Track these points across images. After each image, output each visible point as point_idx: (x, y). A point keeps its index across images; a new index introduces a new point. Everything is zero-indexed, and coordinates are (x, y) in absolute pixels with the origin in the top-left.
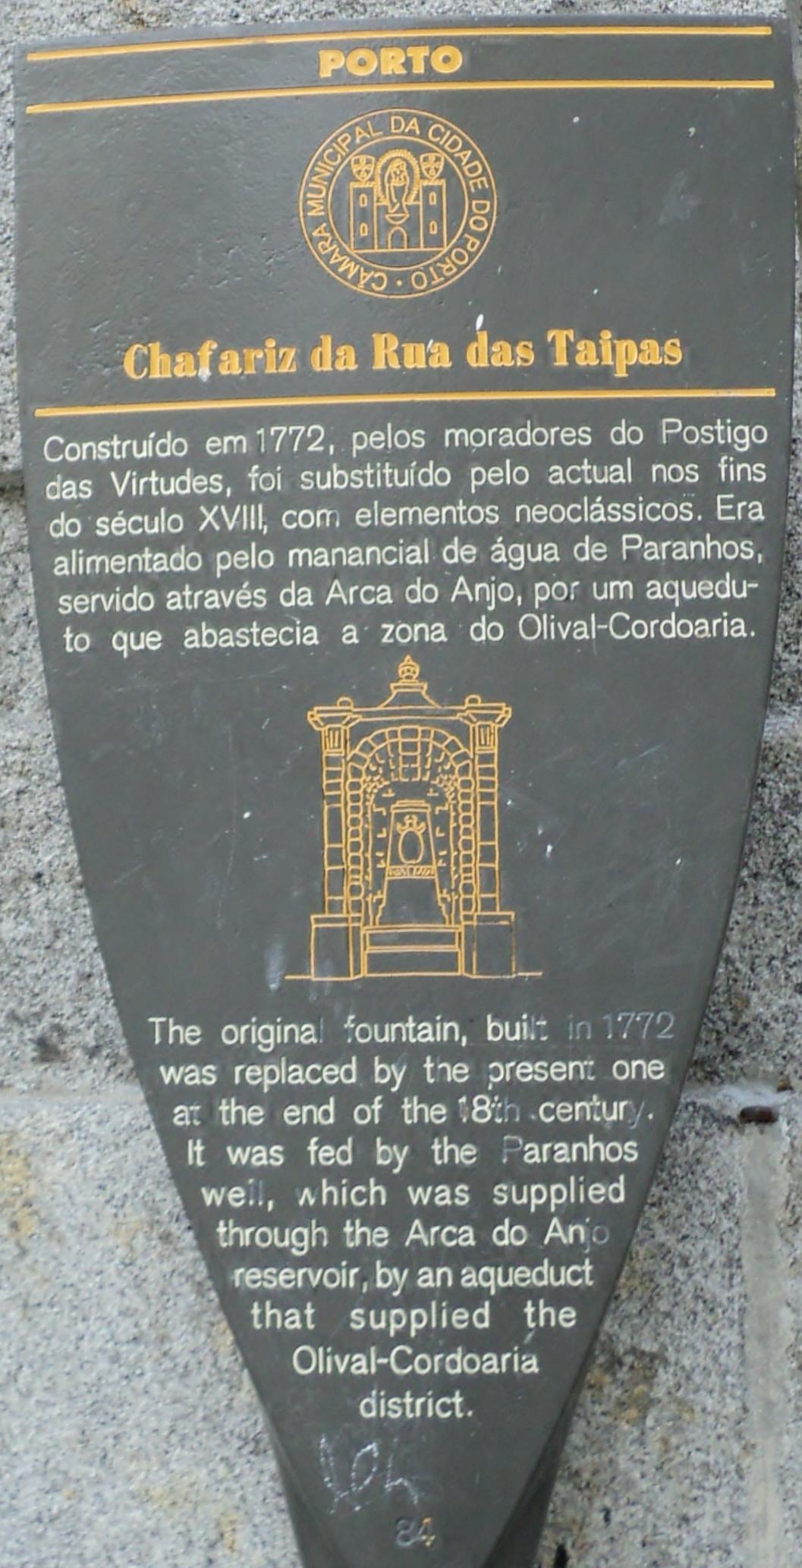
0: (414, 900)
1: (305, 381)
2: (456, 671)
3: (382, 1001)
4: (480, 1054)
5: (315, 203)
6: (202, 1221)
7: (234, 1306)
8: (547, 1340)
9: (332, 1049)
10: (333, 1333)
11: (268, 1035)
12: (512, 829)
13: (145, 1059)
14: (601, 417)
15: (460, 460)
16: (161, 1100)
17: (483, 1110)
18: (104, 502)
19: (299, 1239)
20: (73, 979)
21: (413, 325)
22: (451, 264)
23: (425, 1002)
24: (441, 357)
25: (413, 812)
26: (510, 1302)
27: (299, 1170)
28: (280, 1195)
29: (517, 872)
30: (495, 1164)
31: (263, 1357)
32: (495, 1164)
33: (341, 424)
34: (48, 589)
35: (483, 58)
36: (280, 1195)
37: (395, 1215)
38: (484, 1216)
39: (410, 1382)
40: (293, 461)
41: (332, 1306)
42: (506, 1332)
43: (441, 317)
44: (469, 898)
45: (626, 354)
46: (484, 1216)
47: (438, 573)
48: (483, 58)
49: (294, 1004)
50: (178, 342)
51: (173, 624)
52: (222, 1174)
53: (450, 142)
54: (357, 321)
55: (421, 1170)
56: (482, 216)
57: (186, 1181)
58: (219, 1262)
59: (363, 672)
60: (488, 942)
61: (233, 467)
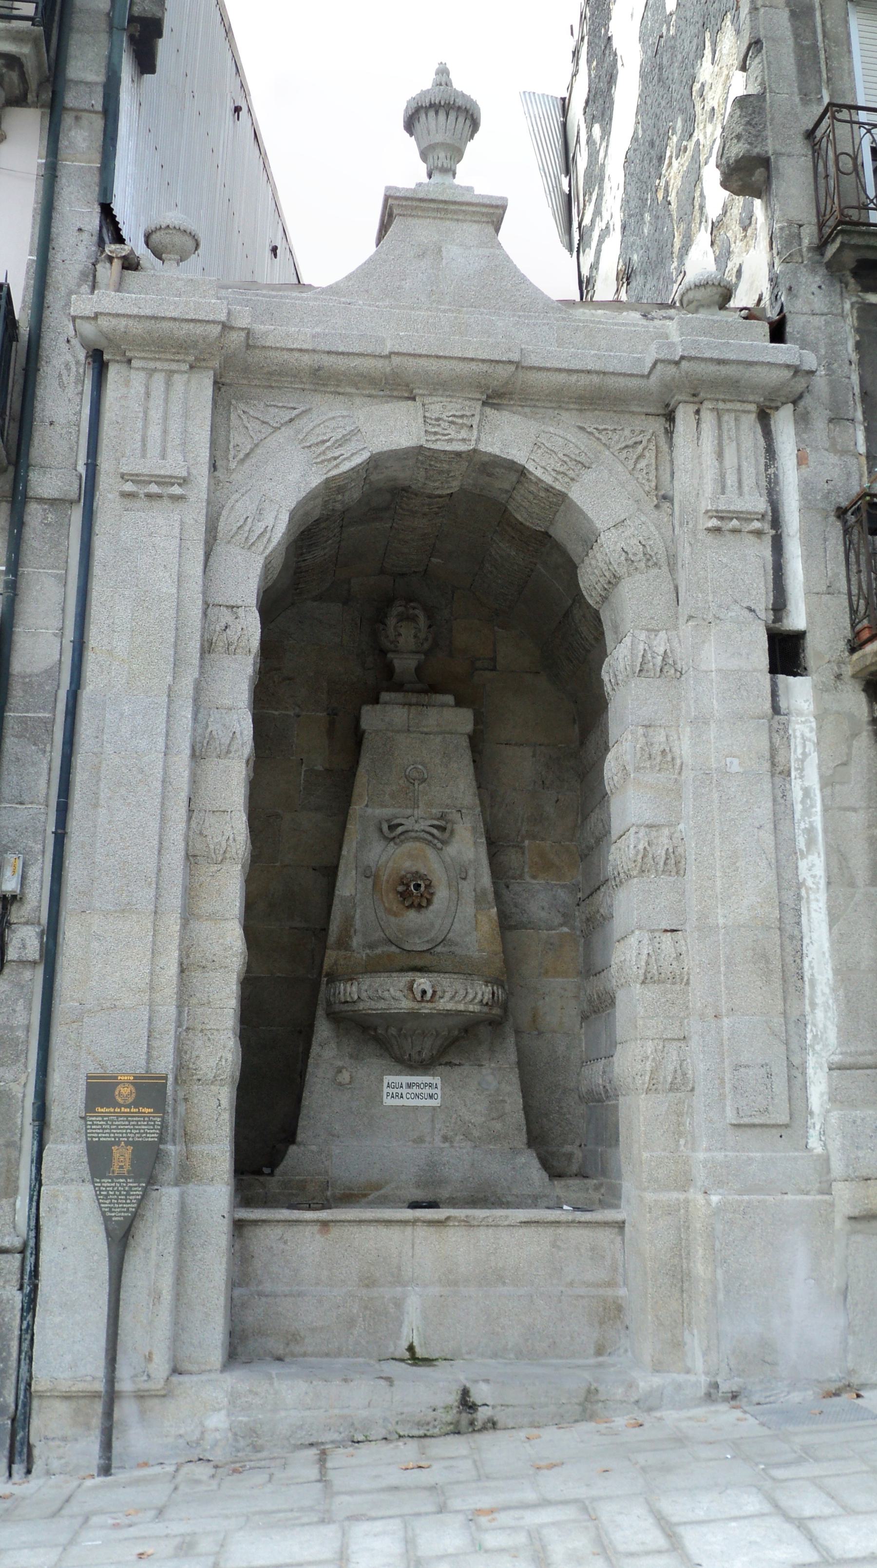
0: (121, 1167)
1: (114, 1112)
2: (127, 1143)
3: (118, 1177)
4: (127, 1183)
5: (117, 1093)
6: (98, 1200)
7: (101, 1208)
8: (132, 1212)
9: (112, 1182)
10: (111, 1211)
11: (106, 1181)
12: (132, 1160)
13: (93, 1183)
14: (144, 1117)
15: (129, 1121)
16: (95, 1187)
17: (127, 1188)
18: (93, 1124)
19: (108, 1202)
20: (87, 1174)
21: (126, 1106)
22: (130, 1100)
23: (122, 1177)
24: (128, 1110)
25: (122, 1157)
26: (128, 1208)
27: (109, 1194)
28: (106, 1197)
29: (132, 1165)
30: (128, 1194)
31: (103, 1214)
32: (128, 1194)
33: (118, 1117)
34: (87, 1133)
35: (135, 1078)
36: (106, 1197)
37: (117, 1199)
38: (126, 1199)
39: (118, 1216)
40: (112, 1121)
41: (110, 1208)
42: (128, 1211)
43: (128, 1106)
44: (127, 1167)
45: (147, 1110)
46: (126, 1199)
47: (126, 1133)
48: (135, 1078)
49: (109, 1177)
50: (102, 1107)
51: (99, 1138)
52: (100, 1195)
53: (132, 1088)
54: (120, 1106)
55: (120, 1195)
56: (134, 1095)
57: (97, 1195)
58: (100, 1204)
59: (118, 1143)
60: (129, 1172)
61: (106, 1121)
